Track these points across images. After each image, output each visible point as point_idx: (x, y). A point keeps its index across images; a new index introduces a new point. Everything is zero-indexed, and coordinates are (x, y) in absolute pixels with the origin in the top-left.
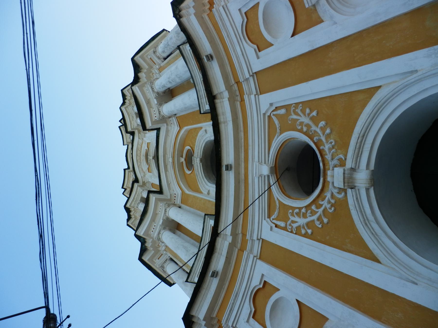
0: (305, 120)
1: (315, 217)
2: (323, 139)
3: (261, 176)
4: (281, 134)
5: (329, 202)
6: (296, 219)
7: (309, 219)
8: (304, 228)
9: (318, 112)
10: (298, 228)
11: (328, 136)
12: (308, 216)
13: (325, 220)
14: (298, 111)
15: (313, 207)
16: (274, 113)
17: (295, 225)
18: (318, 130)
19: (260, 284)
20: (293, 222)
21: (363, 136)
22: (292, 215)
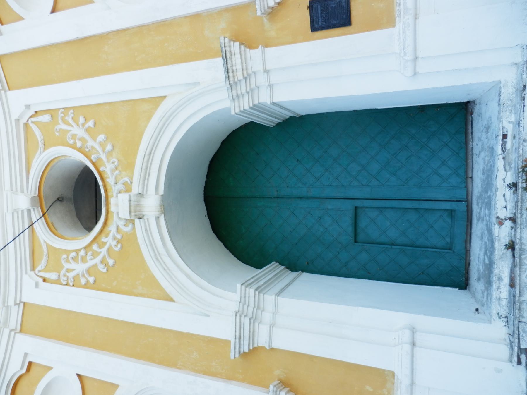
0: (79, 132)
1: (97, 260)
2: (103, 157)
3: (16, 211)
4: (44, 149)
5: (114, 238)
6: (72, 265)
7: (90, 263)
8: (83, 276)
9: (95, 122)
10: (76, 278)
11: (109, 154)
12: (88, 260)
13: (111, 262)
14: (69, 119)
15: (95, 247)
16: (34, 119)
17: (71, 275)
18: (97, 146)
19: (22, 368)
20: (68, 270)
21: (150, 154)
22: (67, 261)
